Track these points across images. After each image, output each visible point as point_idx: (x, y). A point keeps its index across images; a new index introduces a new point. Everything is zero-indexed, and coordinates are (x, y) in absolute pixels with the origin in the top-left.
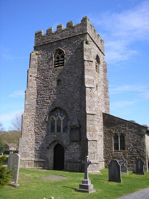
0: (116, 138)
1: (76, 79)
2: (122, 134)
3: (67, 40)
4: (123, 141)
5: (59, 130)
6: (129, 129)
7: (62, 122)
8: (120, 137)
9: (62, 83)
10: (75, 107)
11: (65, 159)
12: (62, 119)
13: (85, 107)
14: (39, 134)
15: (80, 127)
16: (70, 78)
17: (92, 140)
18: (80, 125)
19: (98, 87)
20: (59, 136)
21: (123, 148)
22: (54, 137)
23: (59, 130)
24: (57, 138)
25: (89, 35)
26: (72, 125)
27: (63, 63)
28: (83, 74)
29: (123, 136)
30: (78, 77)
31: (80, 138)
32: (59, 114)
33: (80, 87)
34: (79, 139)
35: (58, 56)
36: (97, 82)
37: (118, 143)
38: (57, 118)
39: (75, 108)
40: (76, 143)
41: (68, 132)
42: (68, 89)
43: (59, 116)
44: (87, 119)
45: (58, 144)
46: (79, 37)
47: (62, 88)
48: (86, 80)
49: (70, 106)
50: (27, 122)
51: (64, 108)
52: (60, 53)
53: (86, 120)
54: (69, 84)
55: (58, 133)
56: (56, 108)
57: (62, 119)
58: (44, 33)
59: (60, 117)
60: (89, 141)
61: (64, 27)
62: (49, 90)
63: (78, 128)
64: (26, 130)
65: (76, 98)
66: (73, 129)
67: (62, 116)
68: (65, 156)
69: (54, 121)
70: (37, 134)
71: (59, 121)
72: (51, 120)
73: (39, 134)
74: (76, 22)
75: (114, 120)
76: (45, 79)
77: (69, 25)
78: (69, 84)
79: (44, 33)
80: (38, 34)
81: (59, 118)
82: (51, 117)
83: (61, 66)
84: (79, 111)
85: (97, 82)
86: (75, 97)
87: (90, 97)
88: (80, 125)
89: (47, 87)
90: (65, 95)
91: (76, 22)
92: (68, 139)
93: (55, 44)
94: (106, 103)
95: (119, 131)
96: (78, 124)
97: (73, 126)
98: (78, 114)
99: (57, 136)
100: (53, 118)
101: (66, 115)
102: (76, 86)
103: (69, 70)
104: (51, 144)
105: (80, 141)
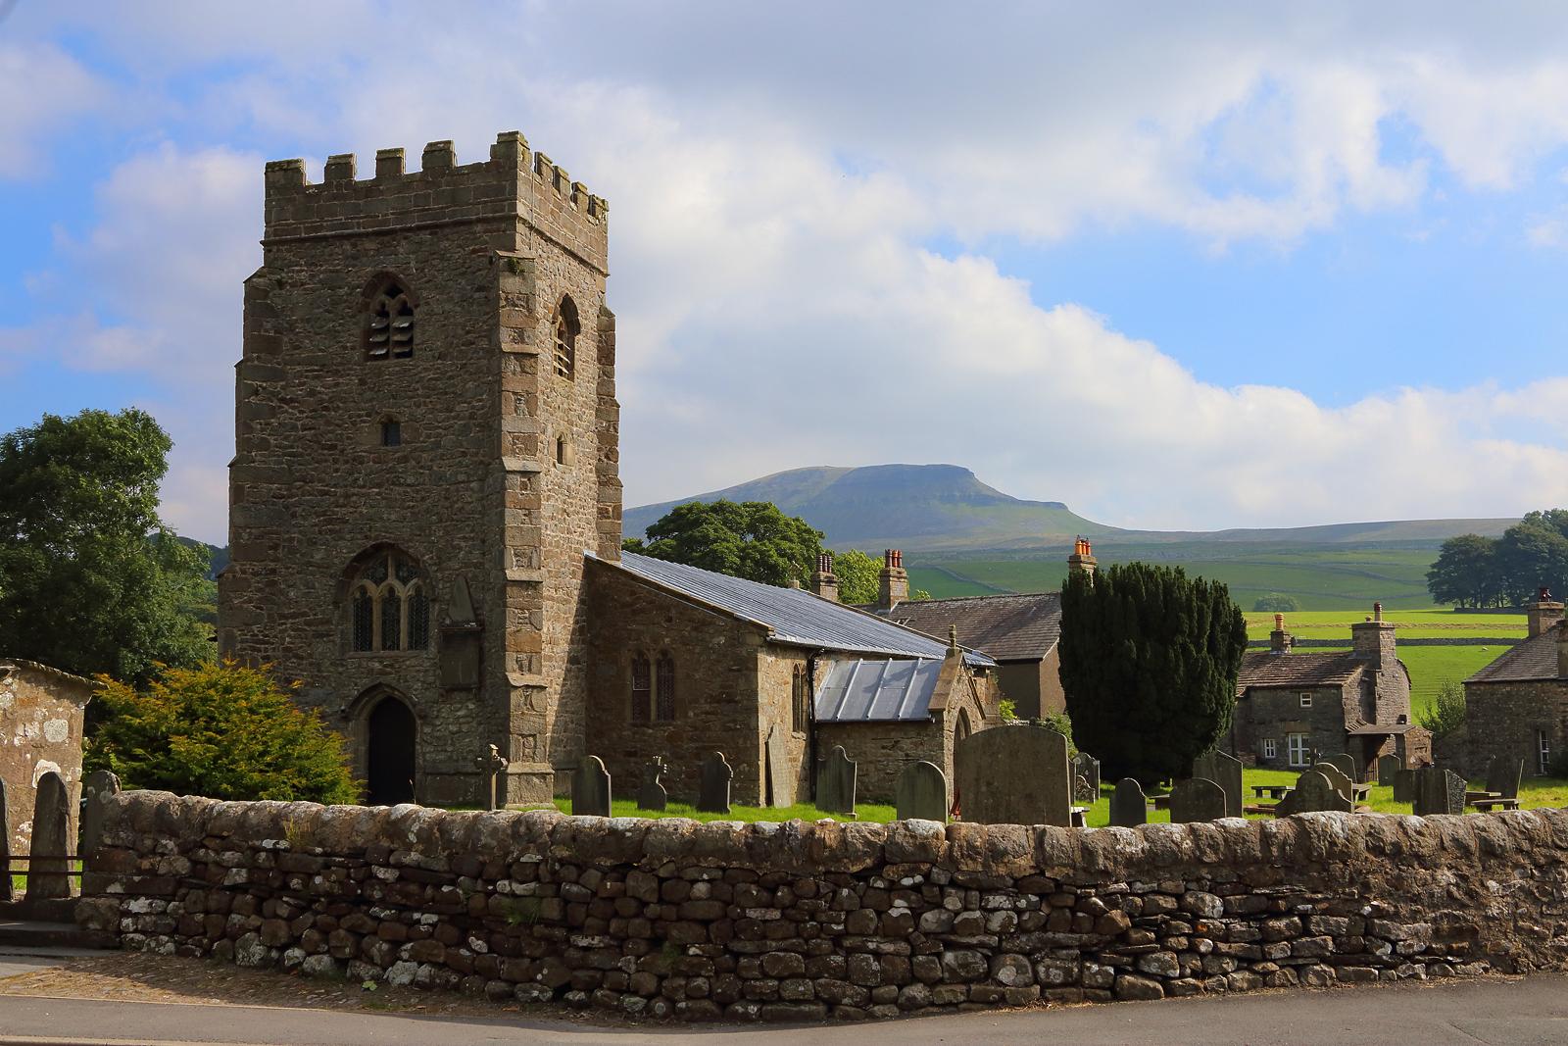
0: (640, 666)
1: (465, 425)
2: (664, 653)
3: (426, 236)
4: (667, 684)
6: (694, 634)
7: (404, 608)
8: (659, 664)
9: (404, 436)
10: (463, 544)
11: (420, 761)
12: (404, 592)
13: (502, 554)
14: (302, 658)
15: (483, 630)
16: (443, 415)
17: (528, 686)
18: (481, 623)
19: (568, 450)
20: (391, 666)
21: (668, 714)
22: (371, 671)
23: (390, 642)
24: (382, 673)
25: (524, 221)
26: (448, 622)
27: (410, 341)
28: (496, 413)
29: (666, 660)
30: (472, 417)
31: (481, 675)
33: (482, 462)
34: (475, 678)
35: (383, 305)
36: (563, 426)
37: (647, 694)
39: (461, 549)
40: (463, 695)
41: (433, 649)
42: (430, 468)
44: (509, 600)
45: (390, 700)
46: (479, 228)
47: (405, 459)
48: (507, 440)
50: (245, 606)
51: (416, 548)
52: (393, 292)
53: (505, 605)
54: (437, 445)
55: (387, 653)
56: (378, 548)
57: (404, 592)
58: (314, 174)
59: (397, 584)
60: (516, 688)
61: (413, 165)
62: (347, 462)
63: (471, 633)
64: (242, 642)
65: (468, 508)
66: (452, 637)
67: (404, 581)
68: (418, 747)
69: (370, 598)
70: (296, 656)
71: (391, 599)
72: (358, 595)
73: (302, 658)
74: (472, 150)
75: (633, 593)
76: (326, 409)
77: (438, 154)
78: (437, 445)
79: (314, 174)
80: (282, 177)
81: (391, 590)
82: (357, 582)
83: (398, 356)
84: (476, 566)
85: (563, 426)
86: (460, 505)
87: (524, 512)
88: (481, 623)
89: (333, 447)
90: (417, 492)
91: (472, 150)
92: (431, 679)
93: (371, 245)
94: (602, 513)
95: (655, 641)
96: (471, 616)
97: (454, 623)
98: (475, 576)
99: (385, 666)
100: (363, 590)
102: (464, 454)
103: (436, 379)
104: (357, 700)
105: (481, 685)
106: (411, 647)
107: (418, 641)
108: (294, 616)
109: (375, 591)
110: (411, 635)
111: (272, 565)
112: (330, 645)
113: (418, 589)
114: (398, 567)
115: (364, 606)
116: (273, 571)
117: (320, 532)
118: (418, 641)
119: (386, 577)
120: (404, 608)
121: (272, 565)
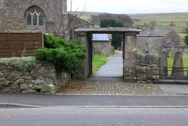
5: (35, 24)
7: (38, 18)
12: (38, 15)
20: (36, 28)
23: (35, 24)
32: (35, 11)
38: (34, 13)
43: (35, 12)
49: (46, 6)
51: (41, 7)
55: (35, 26)
59: (36, 13)
67: (38, 13)
81: (35, 14)
82: (28, 12)
100: (29, 14)
101: (43, 12)
106: (39, 25)
107: (41, 23)
108: (16, 18)
109: (32, 14)
110: (39, 23)
111: (11, 8)
112: (23, 24)
113: (41, 14)
114: (36, 10)
115: (30, 17)
116: (11, 9)
117: (21, 2)
118: (41, 23)
119: (34, 11)
120: (38, 18)
121: (11, 8)
